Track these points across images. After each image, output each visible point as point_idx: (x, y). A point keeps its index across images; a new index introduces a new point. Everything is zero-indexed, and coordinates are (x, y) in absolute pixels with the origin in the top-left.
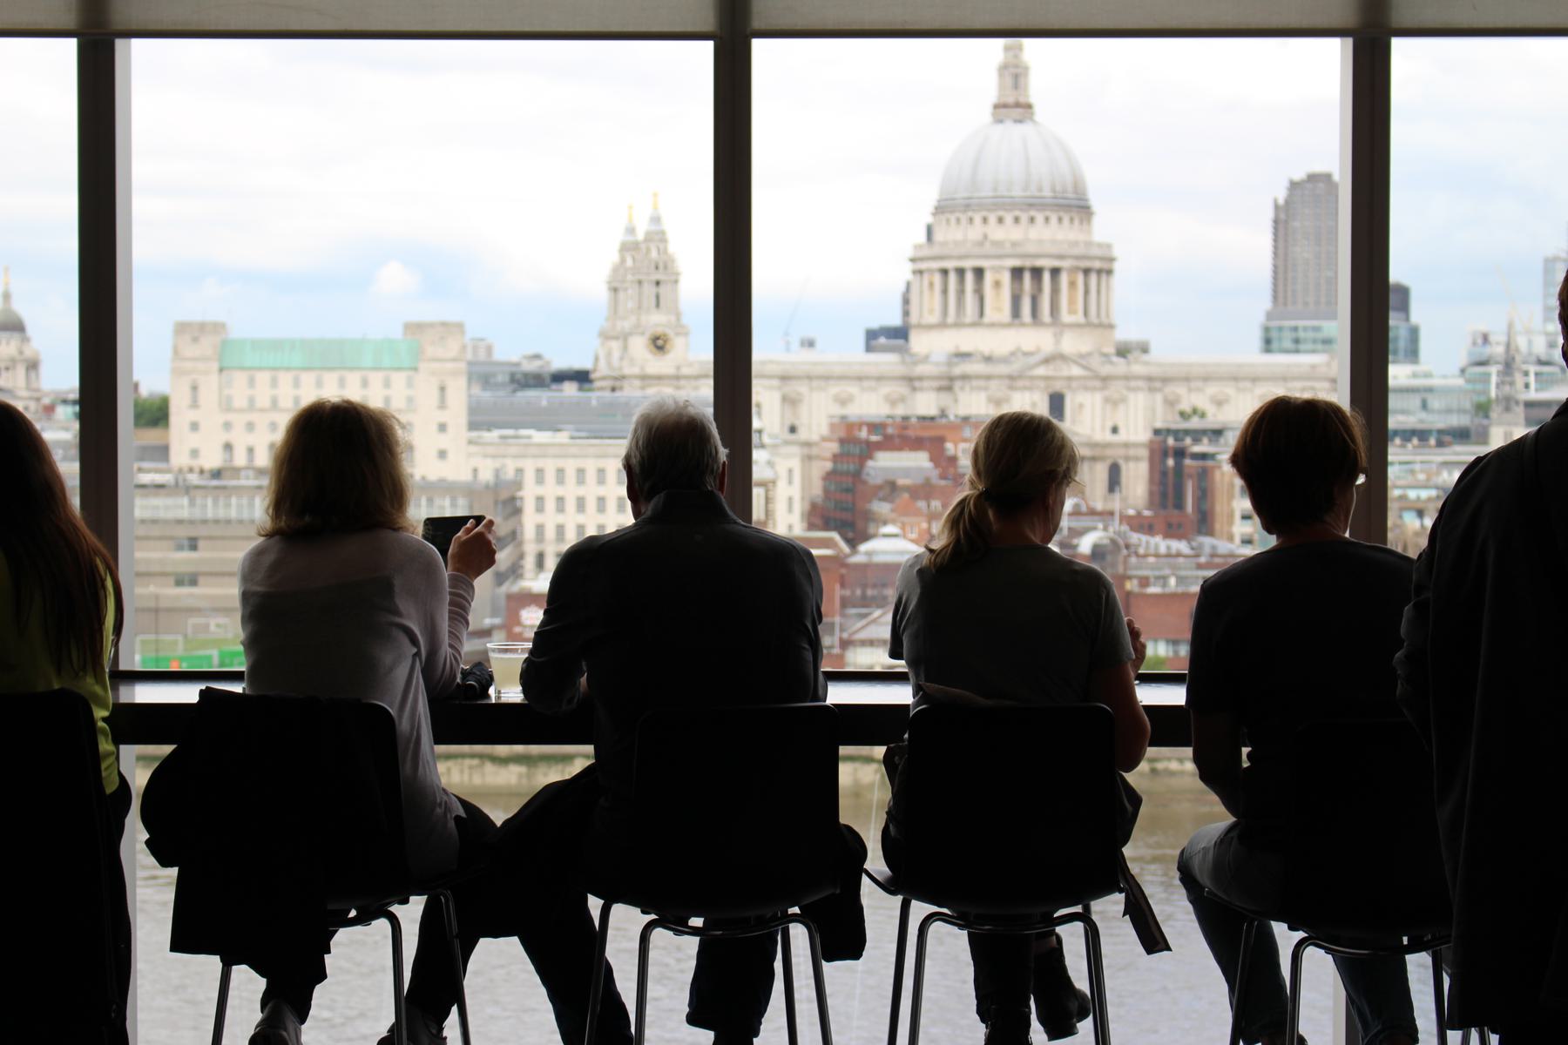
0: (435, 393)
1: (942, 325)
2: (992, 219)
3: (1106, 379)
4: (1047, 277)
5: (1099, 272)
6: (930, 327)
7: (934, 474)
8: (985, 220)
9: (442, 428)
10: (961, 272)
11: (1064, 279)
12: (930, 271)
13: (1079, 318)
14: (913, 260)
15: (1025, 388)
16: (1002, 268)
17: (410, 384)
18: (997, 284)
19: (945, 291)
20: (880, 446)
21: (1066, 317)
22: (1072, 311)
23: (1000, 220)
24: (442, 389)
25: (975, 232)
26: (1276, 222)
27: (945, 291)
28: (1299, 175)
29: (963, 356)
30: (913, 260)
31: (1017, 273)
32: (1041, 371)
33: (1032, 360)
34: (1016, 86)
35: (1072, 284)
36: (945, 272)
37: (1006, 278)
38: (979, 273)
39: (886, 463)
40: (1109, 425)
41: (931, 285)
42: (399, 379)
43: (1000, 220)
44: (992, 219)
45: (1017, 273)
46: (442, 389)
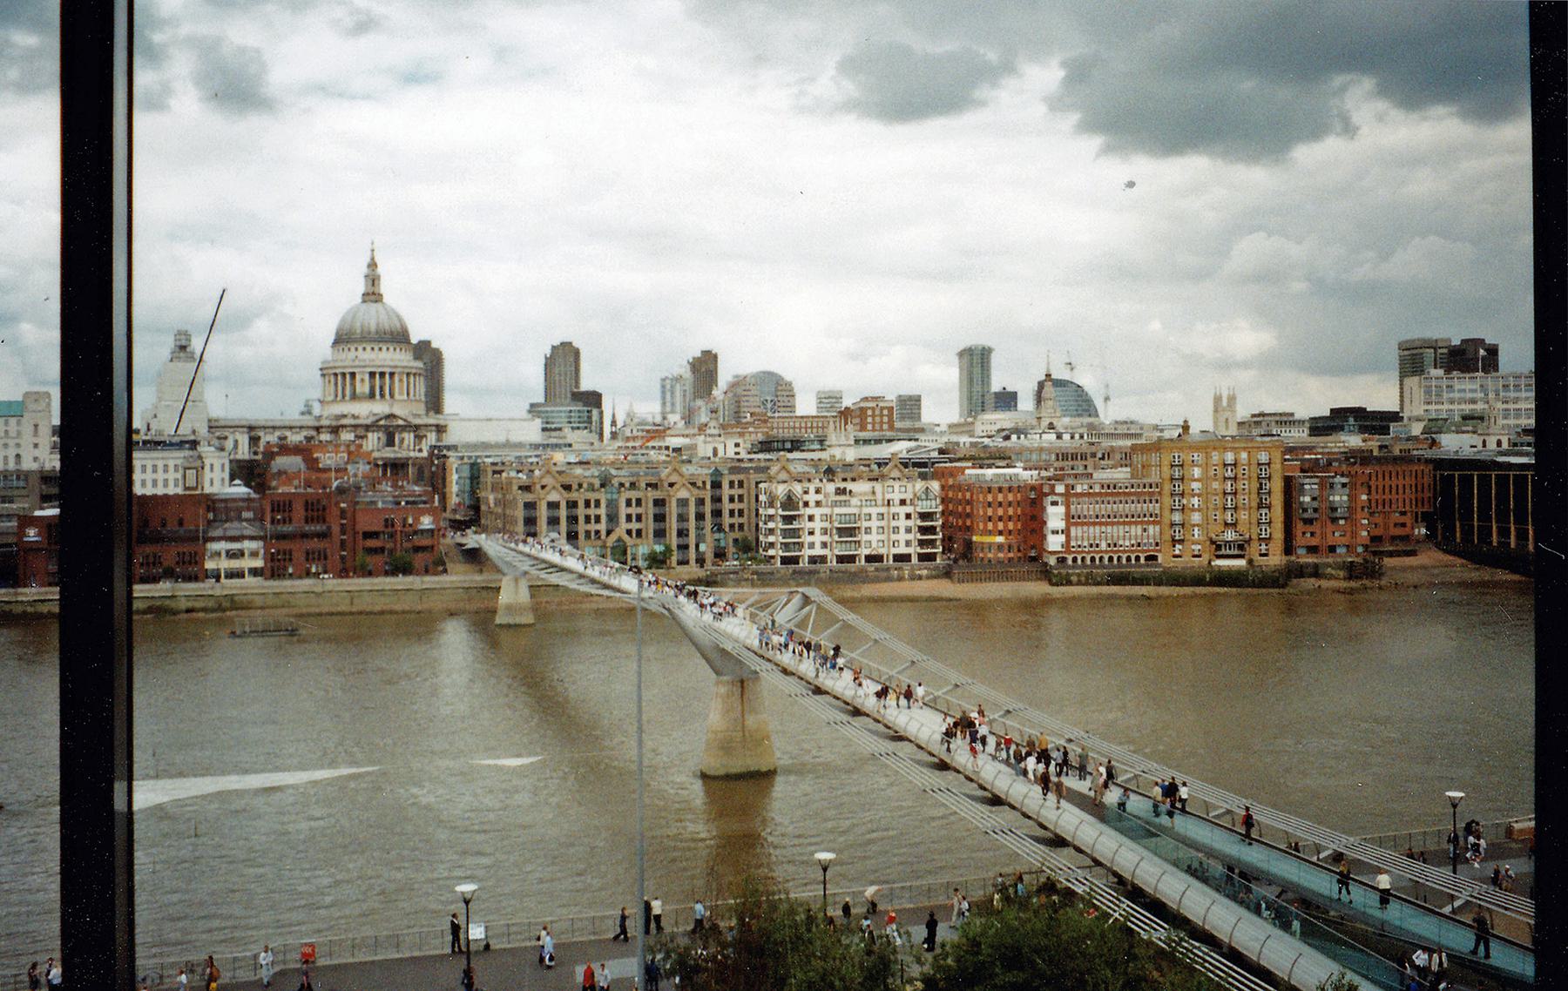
0: (32, 428)
1: (334, 401)
2: (360, 349)
3: (417, 427)
4: (387, 376)
5: (415, 374)
6: (328, 402)
7: (303, 466)
8: (356, 349)
9: (36, 446)
10: (344, 375)
11: (396, 378)
12: (330, 375)
13: (405, 397)
14: (321, 369)
15: (373, 431)
16: (363, 372)
17: (19, 423)
18: (362, 380)
19: (336, 384)
20: (278, 454)
21: (397, 396)
22: (401, 393)
23: (364, 349)
24: (36, 426)
25: (352, 354)
26: (546, 365)
27: (336, 384)
28: (557, 343)
29: (345, 416)
30: (321, 369)
31: (372, 374)
32: (382, 423)
33: (377, 417)
34: (373, 285)
35: (401, 380)
36: (336, 375)
37: (367, 377)
38: (353, 375)
39: (281, 462)
40: (417, 448)
41: (329, 381)
42: (13, 421)
43: (364, 349)
44: (360, 349)
45: (372, 374)
46: (36, 426)
